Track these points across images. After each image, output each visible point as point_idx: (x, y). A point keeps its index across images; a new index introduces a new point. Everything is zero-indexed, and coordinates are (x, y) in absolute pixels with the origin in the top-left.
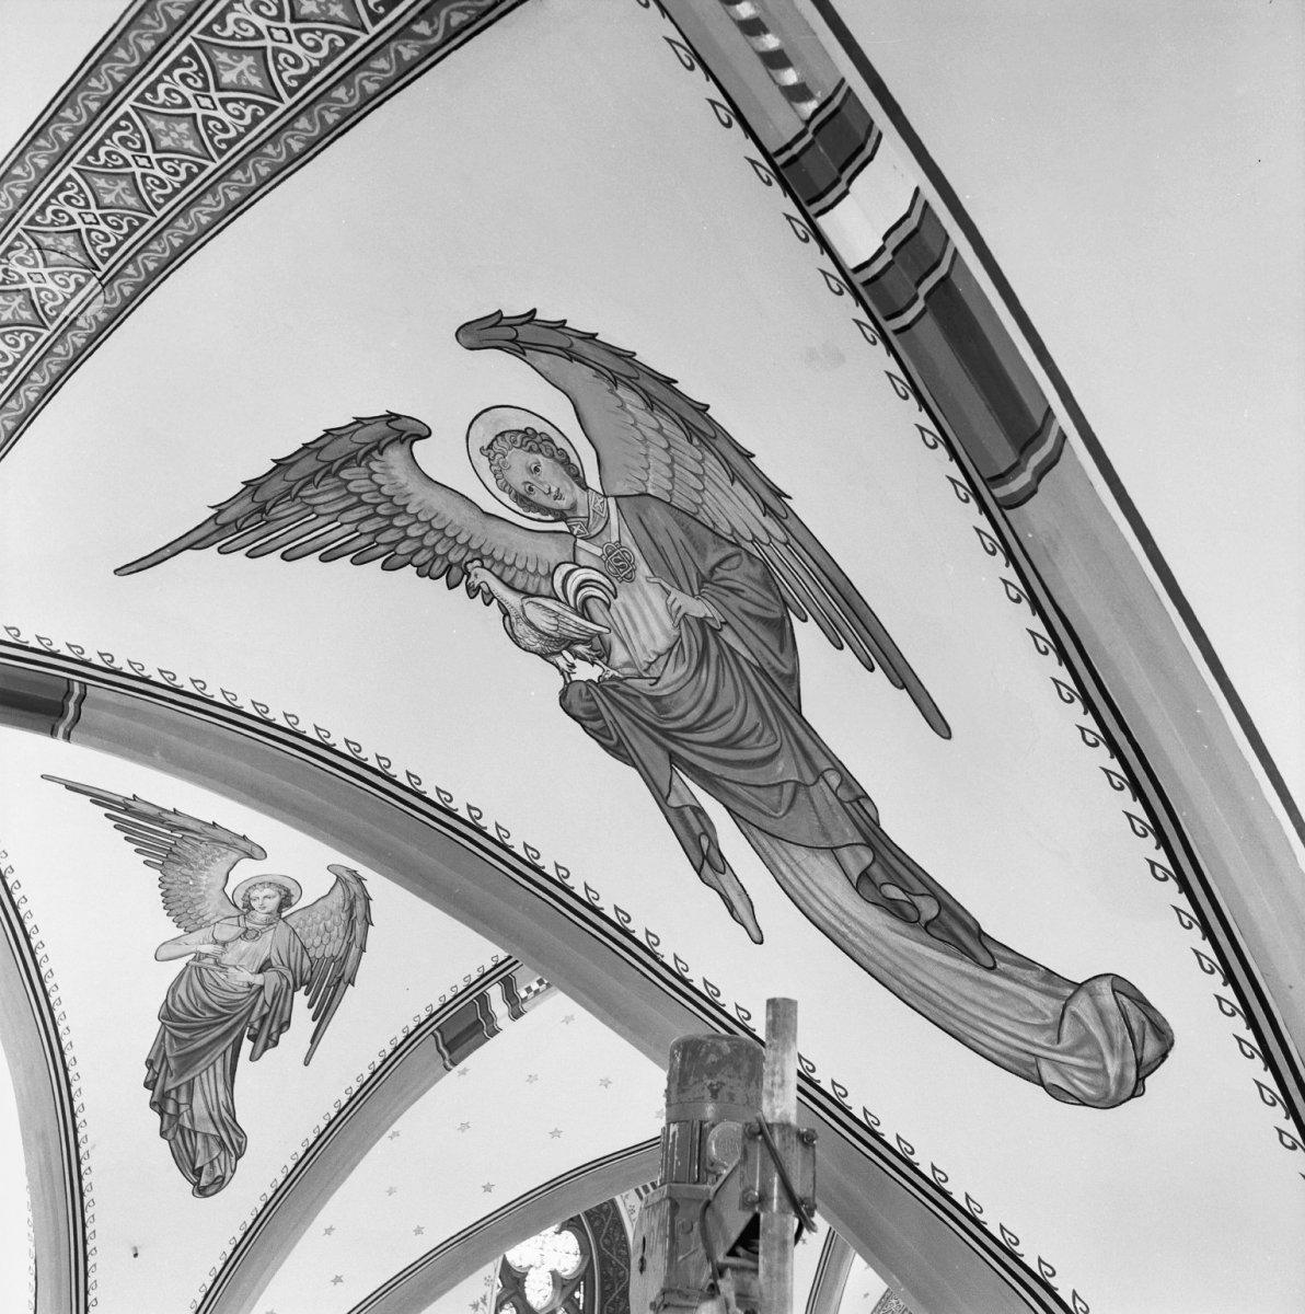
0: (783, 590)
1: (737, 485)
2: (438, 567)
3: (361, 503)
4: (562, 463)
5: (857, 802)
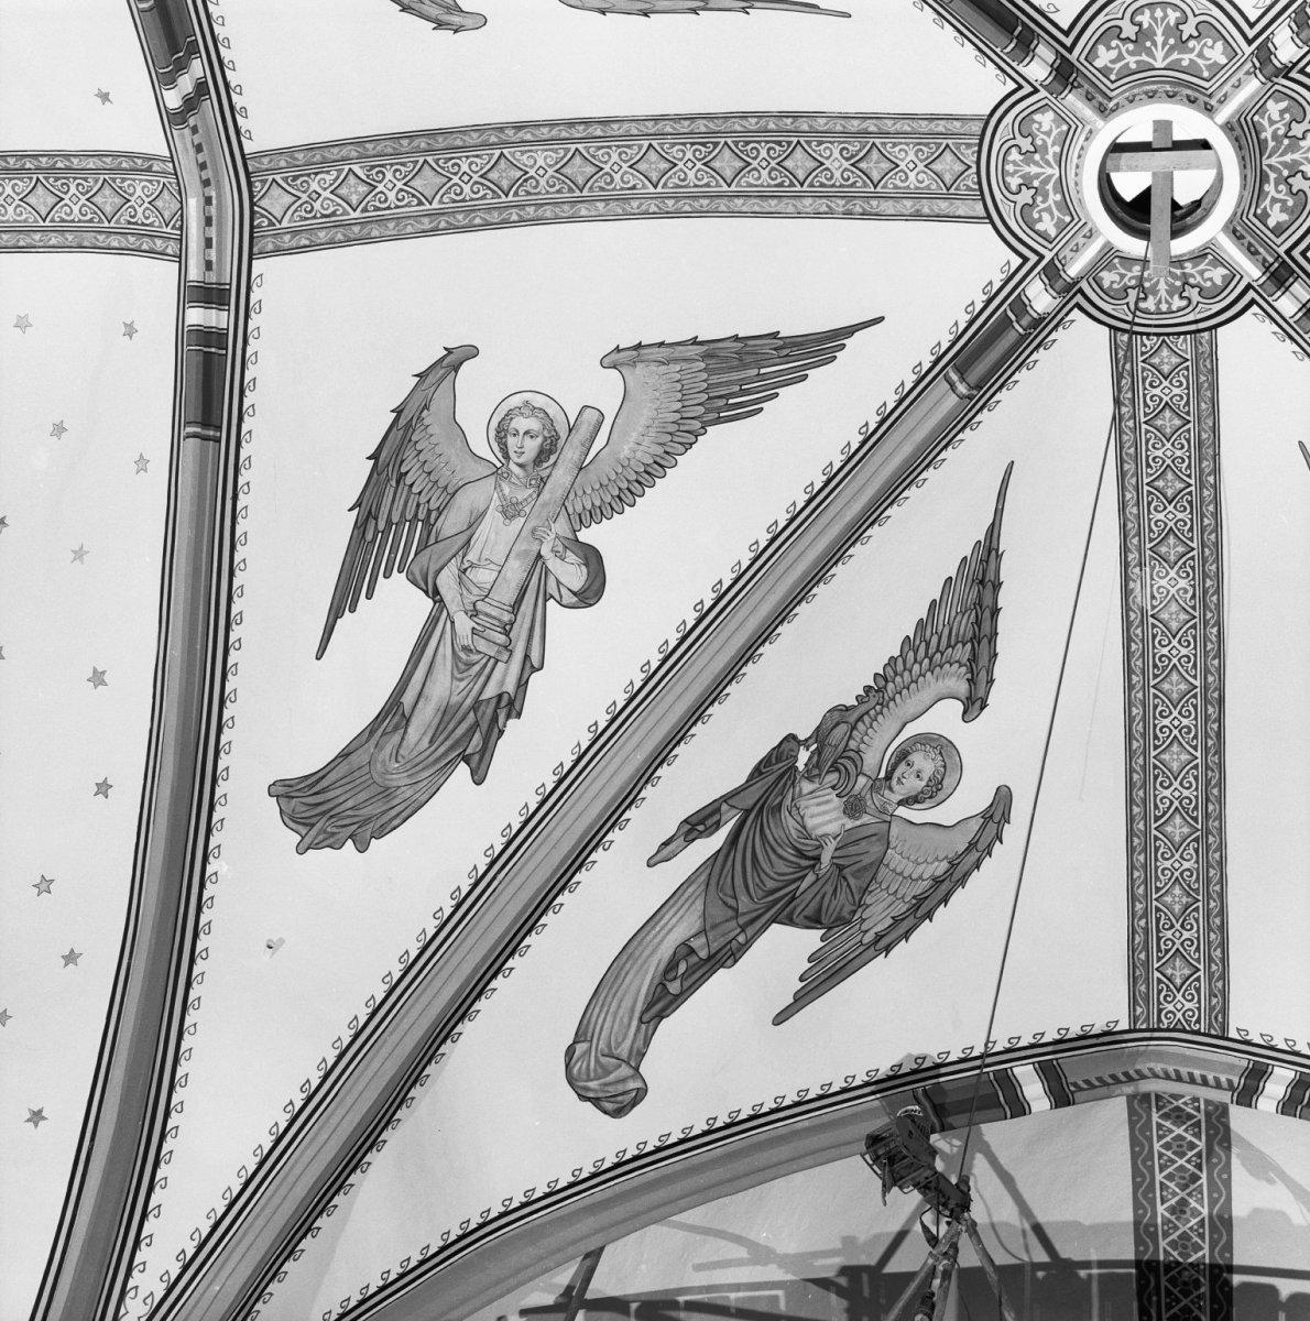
0: (836, 929)
1: (891, 921)
2: (890, 672)
3: (949, 646)
4: (916, 796)
5: (727, 955)
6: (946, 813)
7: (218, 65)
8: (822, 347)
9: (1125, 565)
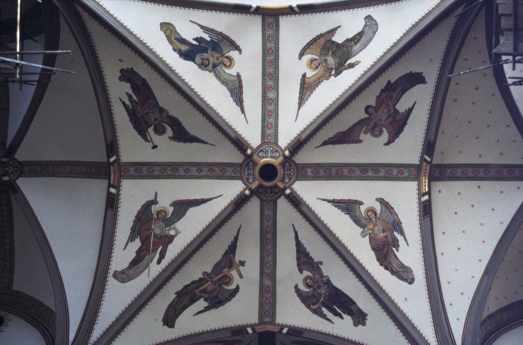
5: (348, 40)
7: (419, 199)
8: (326, 143)
9: (278, 99)
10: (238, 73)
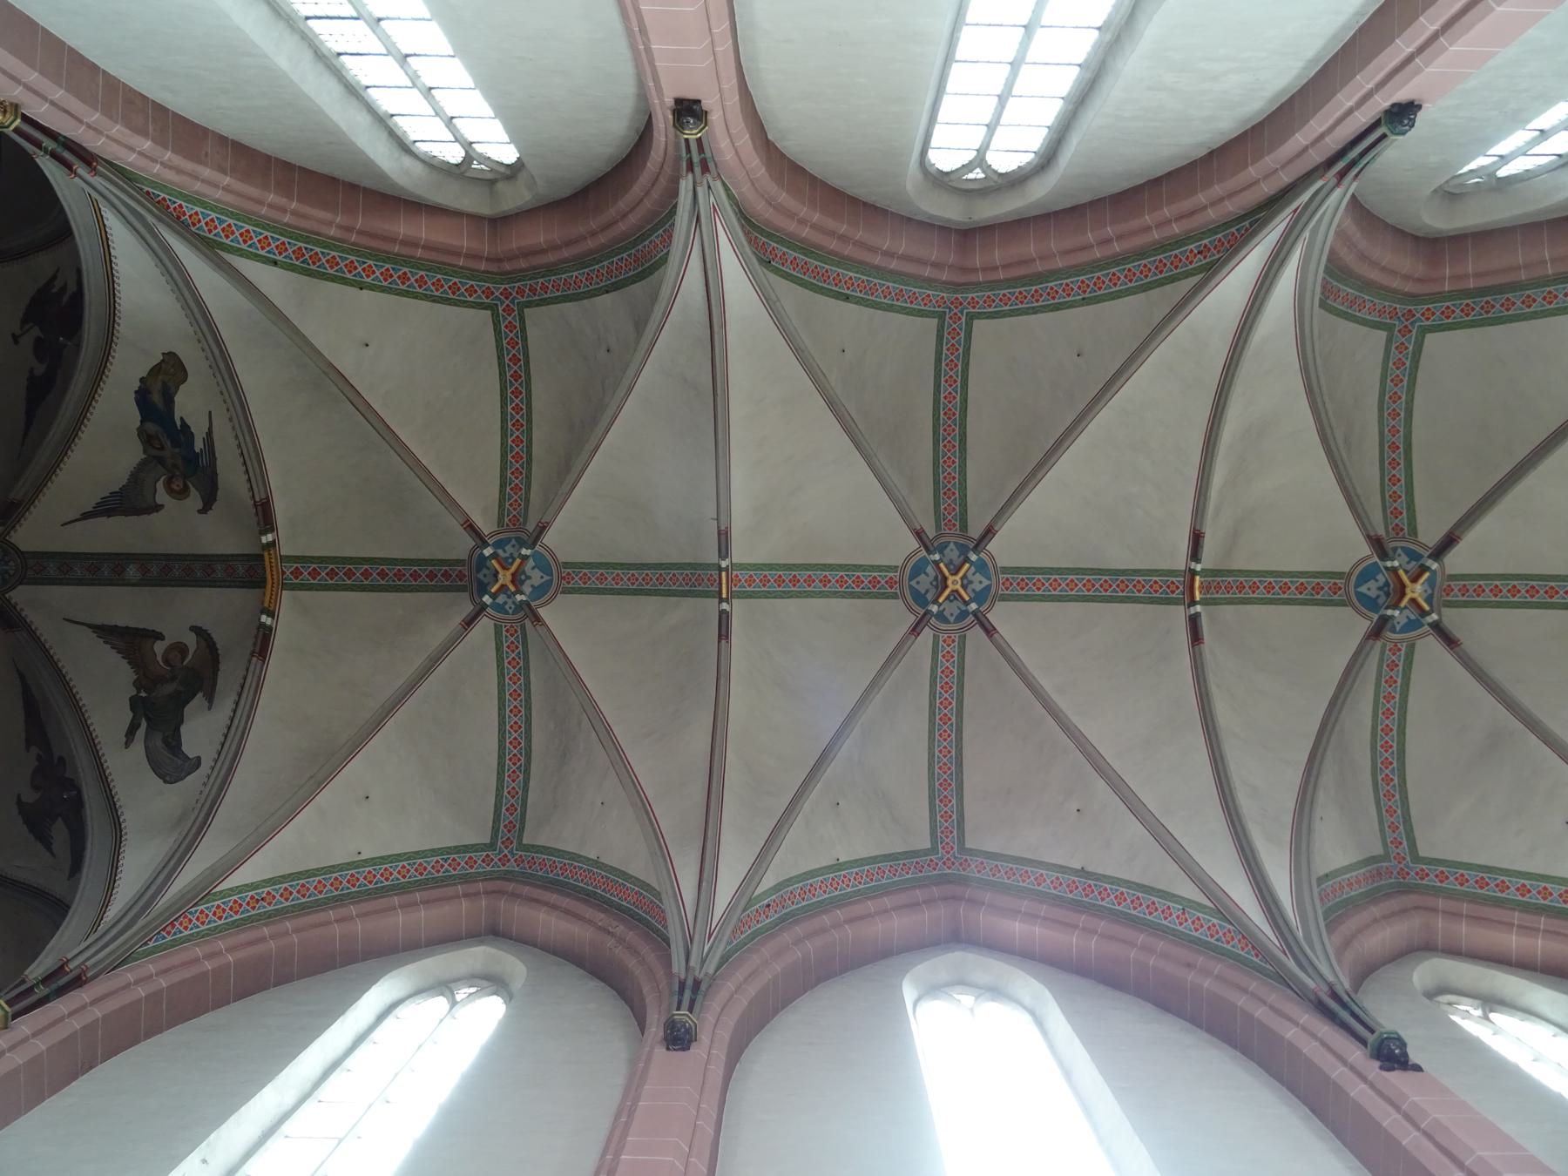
6: (192, 649)
10: (162, 506)
